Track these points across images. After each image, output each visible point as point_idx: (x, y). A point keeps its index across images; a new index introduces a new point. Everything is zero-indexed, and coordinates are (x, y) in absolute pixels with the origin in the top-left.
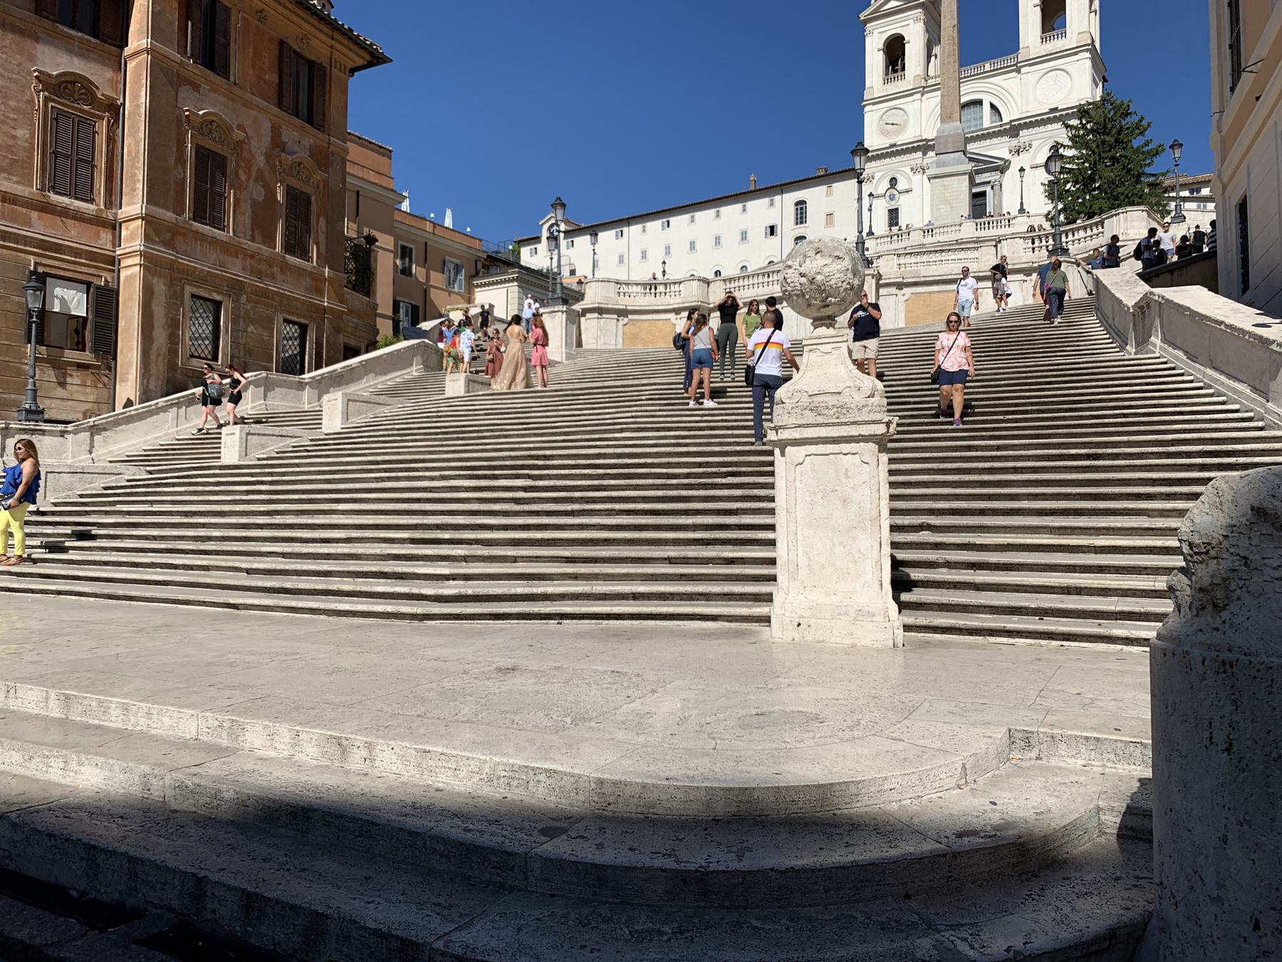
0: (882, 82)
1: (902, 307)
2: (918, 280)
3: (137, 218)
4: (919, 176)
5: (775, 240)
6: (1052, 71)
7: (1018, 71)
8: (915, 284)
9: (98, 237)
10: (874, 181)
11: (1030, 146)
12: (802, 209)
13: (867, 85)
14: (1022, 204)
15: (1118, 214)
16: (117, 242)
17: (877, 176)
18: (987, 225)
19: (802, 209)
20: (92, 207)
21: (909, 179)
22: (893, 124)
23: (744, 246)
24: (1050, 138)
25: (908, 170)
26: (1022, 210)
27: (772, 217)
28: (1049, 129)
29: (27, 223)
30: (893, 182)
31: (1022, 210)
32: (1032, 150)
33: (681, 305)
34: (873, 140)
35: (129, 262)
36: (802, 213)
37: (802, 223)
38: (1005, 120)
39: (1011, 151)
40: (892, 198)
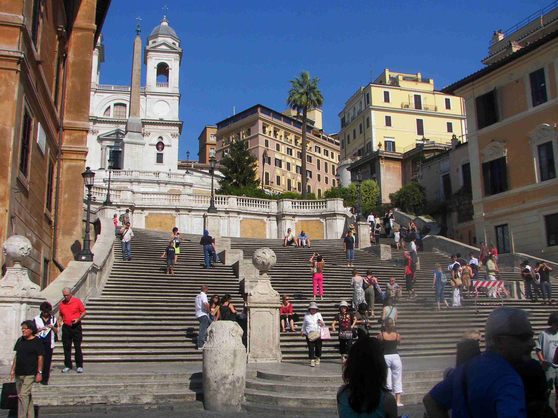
2: (247, 212)
11: (149, 134)
15: (334, 200)
24: (159, 133)
32: (150, 136)
33: (122, 204)
35: (74, 157)
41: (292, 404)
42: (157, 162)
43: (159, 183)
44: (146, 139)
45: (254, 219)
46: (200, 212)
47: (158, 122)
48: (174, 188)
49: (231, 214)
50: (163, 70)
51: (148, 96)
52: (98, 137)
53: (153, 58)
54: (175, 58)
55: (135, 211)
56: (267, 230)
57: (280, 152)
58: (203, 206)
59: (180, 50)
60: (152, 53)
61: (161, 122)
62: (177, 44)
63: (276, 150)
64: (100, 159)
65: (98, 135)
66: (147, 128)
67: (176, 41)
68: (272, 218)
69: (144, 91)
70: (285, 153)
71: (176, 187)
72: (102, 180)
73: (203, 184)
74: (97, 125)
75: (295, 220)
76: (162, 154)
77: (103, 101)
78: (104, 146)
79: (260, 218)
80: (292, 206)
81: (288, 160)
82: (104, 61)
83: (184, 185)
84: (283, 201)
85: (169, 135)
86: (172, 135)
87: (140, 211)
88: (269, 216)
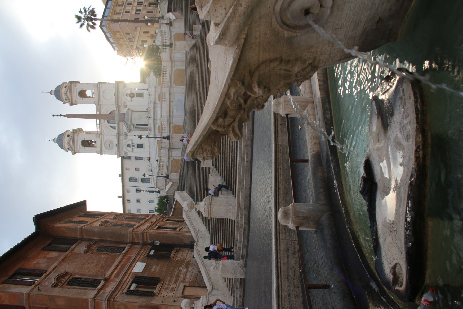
1: (177, 86)
3: (132, 234)
4: (129, 137)
7: (100, 104)
8: (171, 82)
9: (137, 247)
10: (127, 152)
11: (124, 102)
12: (132, 179)
14: (145, 90)
16: (138, 244)
17: (126, 151)
19: (132, 179)
20: (126, 249)
23: (142, 201)
25: (125, 141)
26: (148, 90)
27: (133, 190)
29: (131, 257)
30: (129, 146)
31: (148, 90)
32: (126, 101)
35: (145, 238)
36: (134, 180)
37: (137, 180)
38: (115, 109)
39: (125, 108)
40: (133, 146)
41: (244, 251)
42: (142, 97)
43: (155, 108)
44: (128, 104)
45: (174, 76)
47: (117, 97)
49: (172, 92)
51: (101, 103)
52: (129, 133)
53: (76, 100)
55: (172, 147)
56: (181, 68)
57: (130, 10)
60: (73, 100)
61: (116, 95)
63: (130, 14)
66: (121, 103)
67: (63, 86)
68: (173, 65)
70: (130, 7)
72: (155, 141)
74: (121, 133)
76: (137, 94)
78: (134, 129)
79: (173, 72)
81: (136, 4)
83: (155, 92)
86: (124, 88)
87: (172, 145)
88: (172, 67)
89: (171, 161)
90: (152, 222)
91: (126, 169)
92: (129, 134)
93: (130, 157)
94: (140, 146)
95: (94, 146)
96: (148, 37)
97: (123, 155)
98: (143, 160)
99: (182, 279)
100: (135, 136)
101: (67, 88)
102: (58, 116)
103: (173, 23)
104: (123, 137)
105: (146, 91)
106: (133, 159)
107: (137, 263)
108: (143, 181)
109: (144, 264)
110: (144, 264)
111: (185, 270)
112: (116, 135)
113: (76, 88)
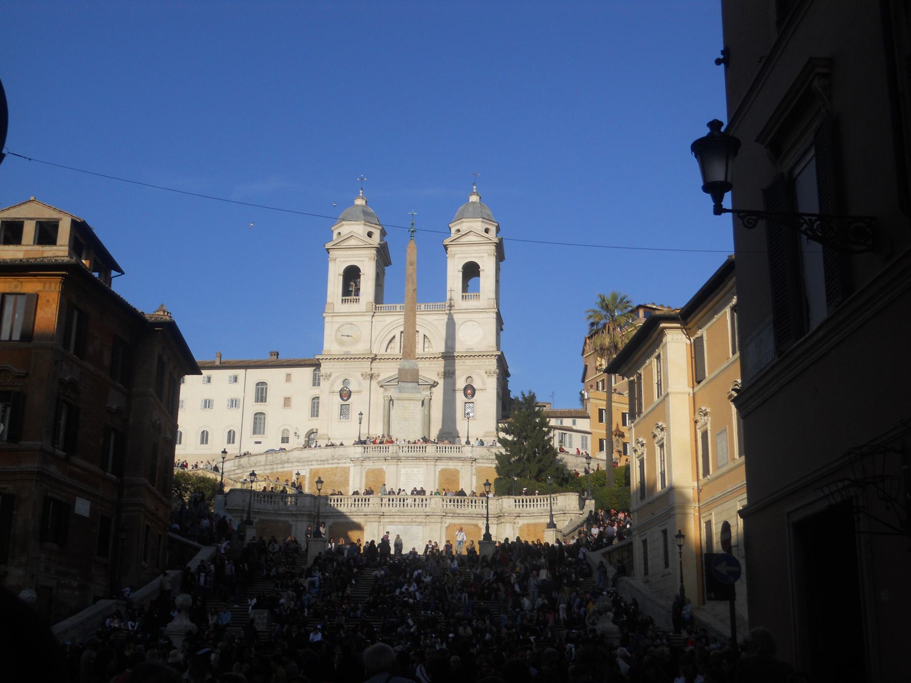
0: (341, 301)
1: (444, 530)
5: (236, 413)
6: (472, 321)
10: (331, 379)
12: (262, 389)
13: (329, 300)
14: (468, 437)
18: (444, 449)
21: (360, 384)
22: (348, 336)
25: (360, 374)
27: (236, 391)
28: (467, 364)
33: (298, 512)
34: (331, 345)
36: (262, 393)
37: (262, 401)
46: (394, 518)
48: (448, 467)
50: (471, 271)
54: (489, 252)
58: (398, 510)
59: (496, 240)
62: (493, 229)
64: (382, 418)
65: (380, 379)
67: (490, 224)
69: (444, 309)
71: (451, 465)
72: (349, 460)
73: (491, 457)
75: (518, 523)
77: (386, 328)
78: (387, 396)
80: (516, 505)
82: (391, 264)
84: (502, 498)
85: (482, 373)
86: (486, 373)
89: (287, 519)
90: (157, 510)
91: (289, 375)
92: (374, 383)
93: (319, 385)
94: (344, 411)
95: (347, 298)
96: (618, 425)
97: (325, 368)
98: (310, 418)
99: (62, 582)
100: (361, 414)
101: (485, 235)
102: (413, 224)
103: (552, 529)
104: (368, 371)
105: (466, 440)
106: (315, 391)
107: (90, 502)
108: (258, 416)
109: (87, 515)
110: (87, 515)
111: (75, 584)
112: (374, 352)
113: (486, 254)
